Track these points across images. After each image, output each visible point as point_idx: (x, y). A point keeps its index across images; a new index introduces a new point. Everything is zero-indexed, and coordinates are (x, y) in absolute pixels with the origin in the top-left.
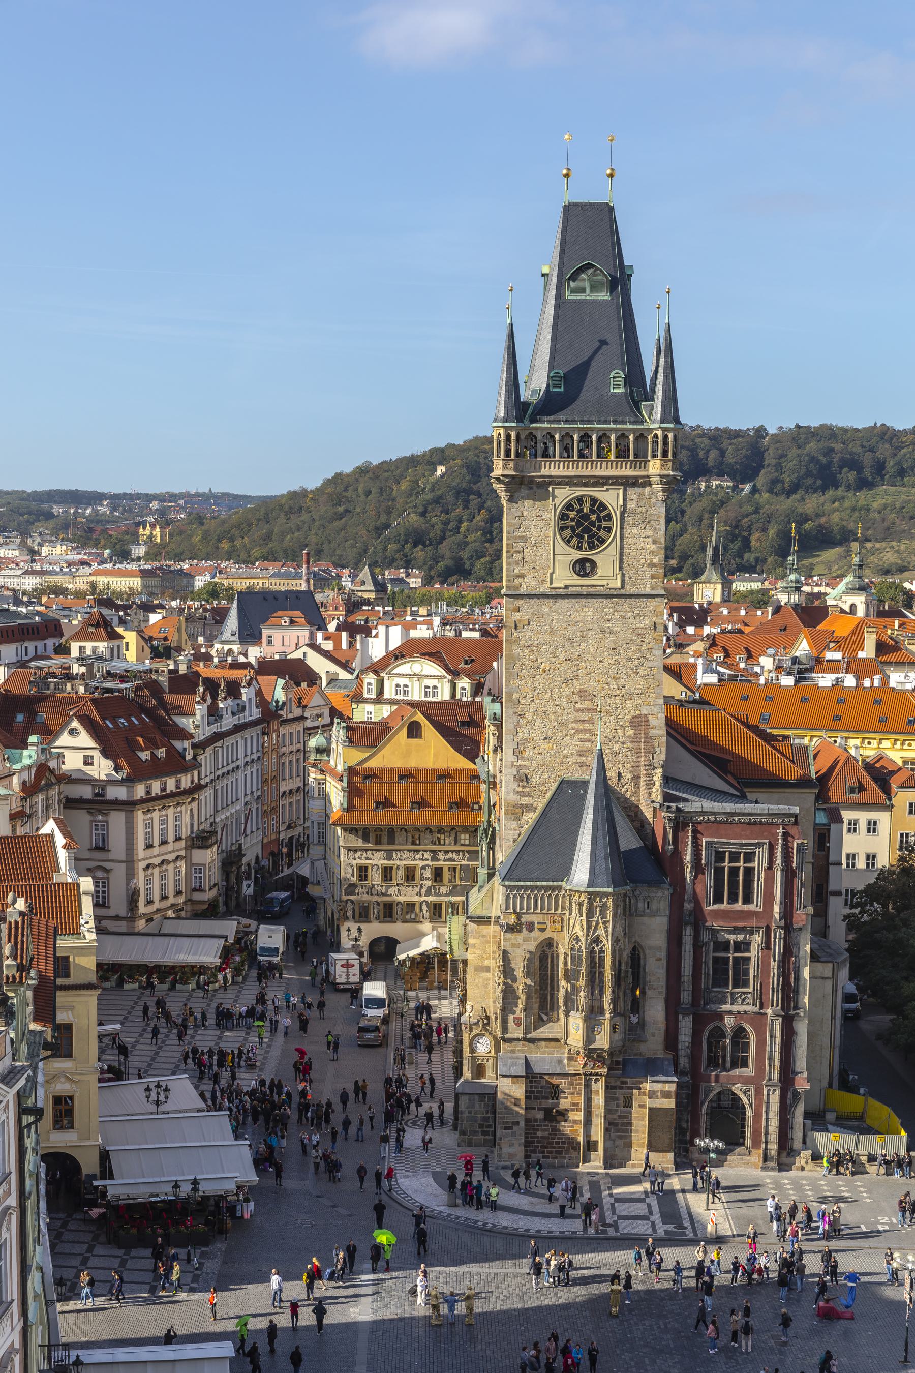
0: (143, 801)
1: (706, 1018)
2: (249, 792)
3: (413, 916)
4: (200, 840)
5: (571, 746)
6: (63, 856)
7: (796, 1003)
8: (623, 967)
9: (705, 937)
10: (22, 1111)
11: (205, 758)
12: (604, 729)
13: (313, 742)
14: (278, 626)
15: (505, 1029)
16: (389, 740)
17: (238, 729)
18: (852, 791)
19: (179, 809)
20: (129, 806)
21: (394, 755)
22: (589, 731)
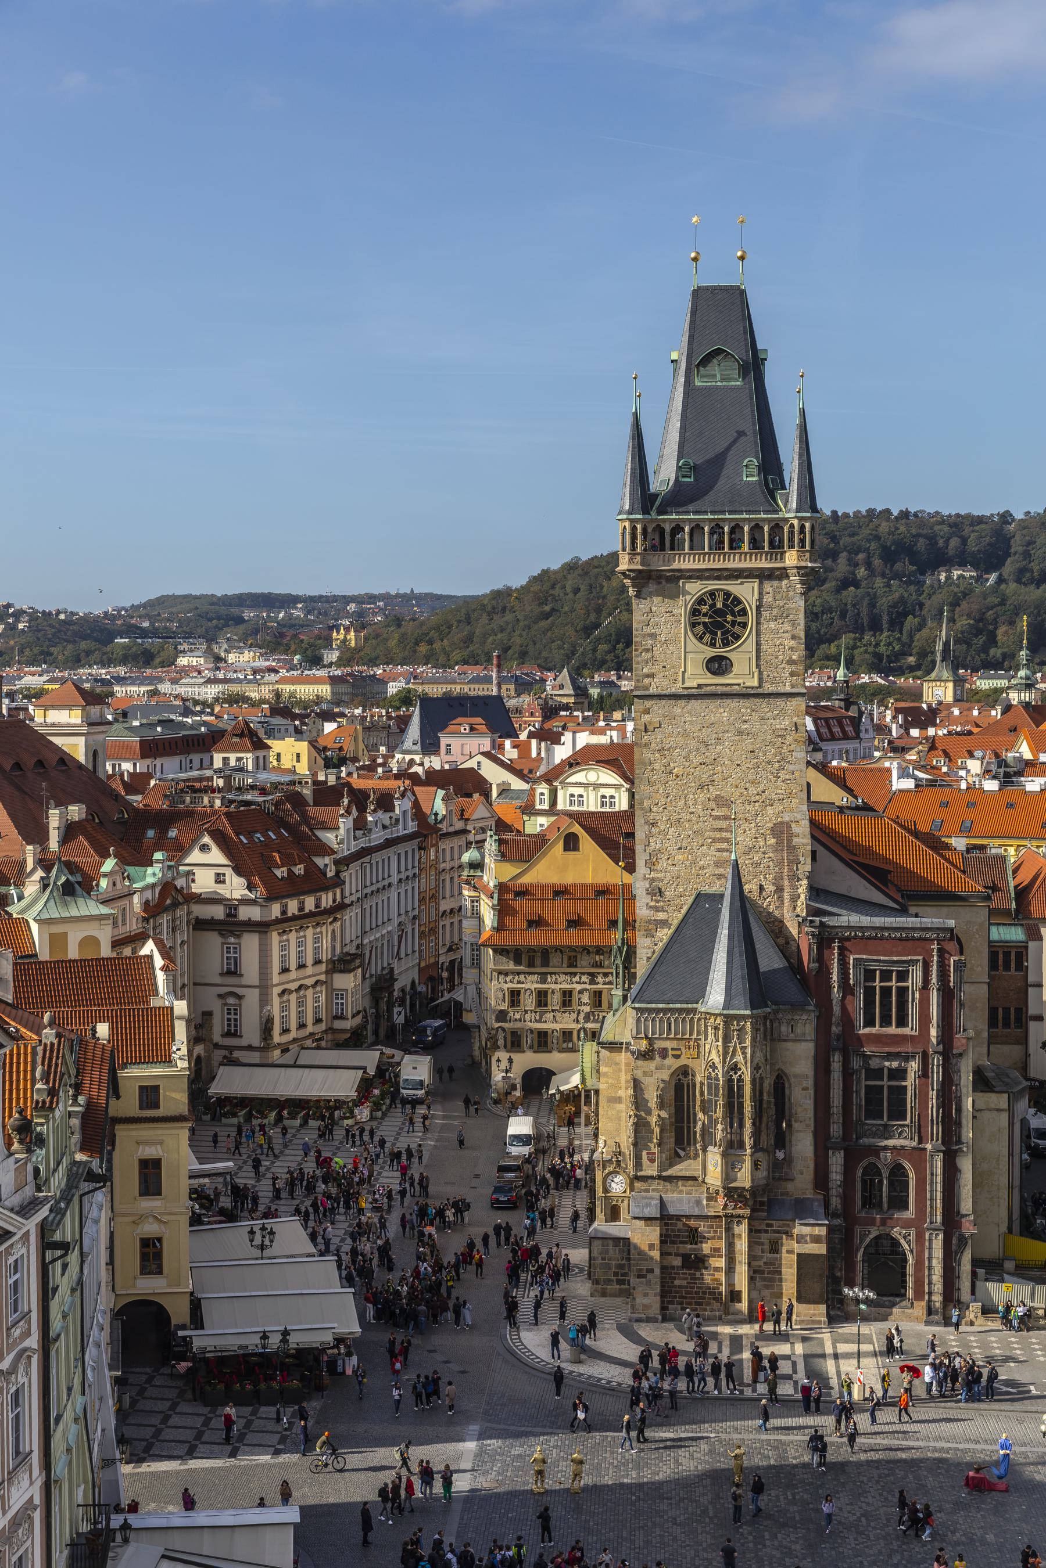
0: (277, 921)
1: (855, 1154)
4: (342, 963)
5: (708, 856)
6: (161, 977)
7: (960, 1137)
8: (765, 1097)
9: (856, 1063)
10: (46, 1244)
11: (352, 876)
12: (743, 837)
13: (466, 857)
14: (456, 734)
15: (638, 1165)
16: (544, 854)
17: (389, 843)
20: (262, 927)
21: (550, 869)
22: (727, 840)
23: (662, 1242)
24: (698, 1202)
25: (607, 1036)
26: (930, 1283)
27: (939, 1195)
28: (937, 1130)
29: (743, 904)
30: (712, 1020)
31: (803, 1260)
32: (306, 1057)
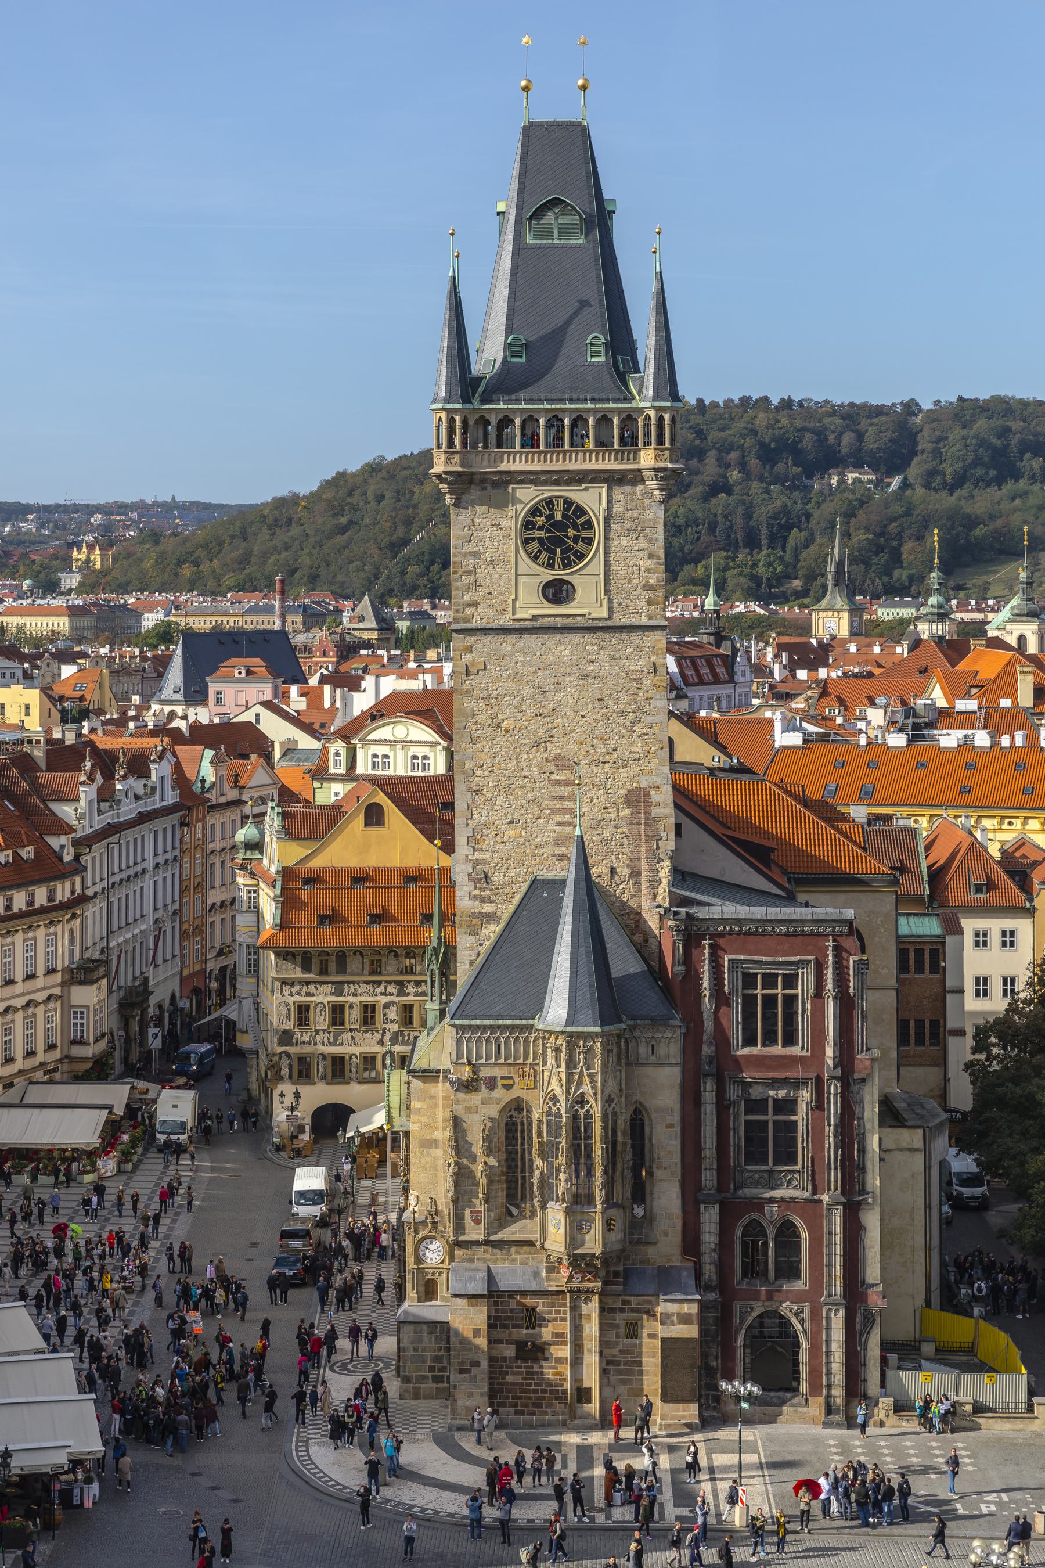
2: (160, 905)
3: (373, 1074)
4: (83, 973)
5: (546, 832)
7: (863, 1185)
8: (620, 1138)
9: (733, 1092)
11: (95, 859)
13: (241, 835)
14: (229, 678)
15: (460, 1227)
16: (341, 831)
17: (143, 818)
18: (979, 889)
19: (52, 930)
21: (348, 850)
22: (571, 812)
23: (490, 1326)
24: (536, 1274)
25: (419, 1061)
26: (829, 1373)
27: (839, 1260)
28: (835, 1176)
29: (590, 892)
30: (552, 1040)
31: (667, 1344)
32: (35, 1094)
